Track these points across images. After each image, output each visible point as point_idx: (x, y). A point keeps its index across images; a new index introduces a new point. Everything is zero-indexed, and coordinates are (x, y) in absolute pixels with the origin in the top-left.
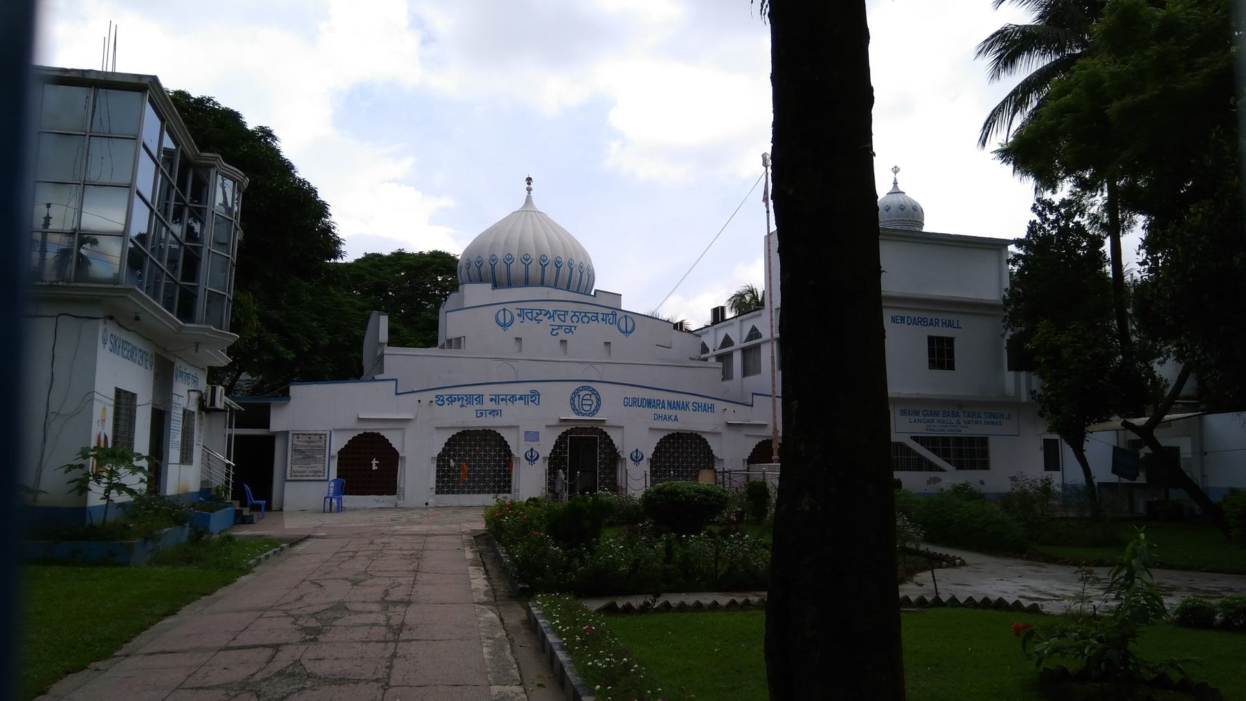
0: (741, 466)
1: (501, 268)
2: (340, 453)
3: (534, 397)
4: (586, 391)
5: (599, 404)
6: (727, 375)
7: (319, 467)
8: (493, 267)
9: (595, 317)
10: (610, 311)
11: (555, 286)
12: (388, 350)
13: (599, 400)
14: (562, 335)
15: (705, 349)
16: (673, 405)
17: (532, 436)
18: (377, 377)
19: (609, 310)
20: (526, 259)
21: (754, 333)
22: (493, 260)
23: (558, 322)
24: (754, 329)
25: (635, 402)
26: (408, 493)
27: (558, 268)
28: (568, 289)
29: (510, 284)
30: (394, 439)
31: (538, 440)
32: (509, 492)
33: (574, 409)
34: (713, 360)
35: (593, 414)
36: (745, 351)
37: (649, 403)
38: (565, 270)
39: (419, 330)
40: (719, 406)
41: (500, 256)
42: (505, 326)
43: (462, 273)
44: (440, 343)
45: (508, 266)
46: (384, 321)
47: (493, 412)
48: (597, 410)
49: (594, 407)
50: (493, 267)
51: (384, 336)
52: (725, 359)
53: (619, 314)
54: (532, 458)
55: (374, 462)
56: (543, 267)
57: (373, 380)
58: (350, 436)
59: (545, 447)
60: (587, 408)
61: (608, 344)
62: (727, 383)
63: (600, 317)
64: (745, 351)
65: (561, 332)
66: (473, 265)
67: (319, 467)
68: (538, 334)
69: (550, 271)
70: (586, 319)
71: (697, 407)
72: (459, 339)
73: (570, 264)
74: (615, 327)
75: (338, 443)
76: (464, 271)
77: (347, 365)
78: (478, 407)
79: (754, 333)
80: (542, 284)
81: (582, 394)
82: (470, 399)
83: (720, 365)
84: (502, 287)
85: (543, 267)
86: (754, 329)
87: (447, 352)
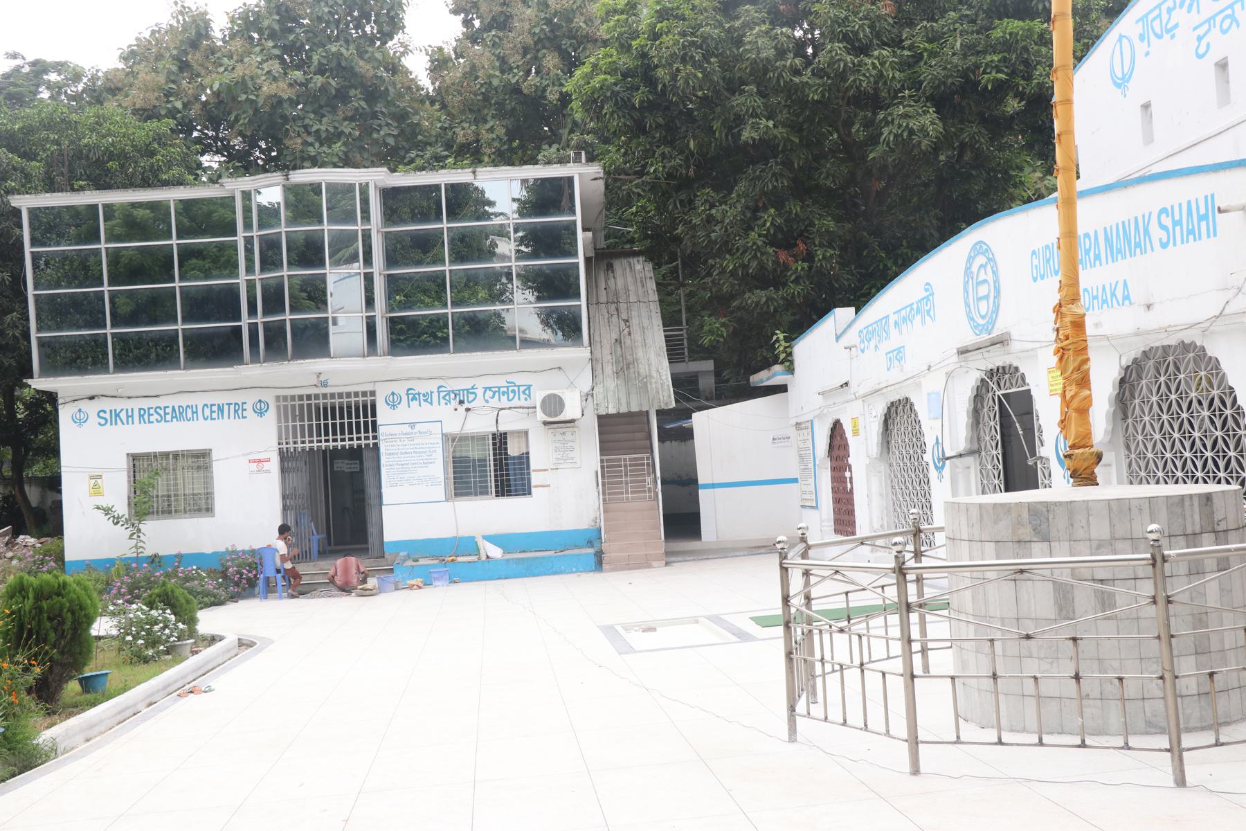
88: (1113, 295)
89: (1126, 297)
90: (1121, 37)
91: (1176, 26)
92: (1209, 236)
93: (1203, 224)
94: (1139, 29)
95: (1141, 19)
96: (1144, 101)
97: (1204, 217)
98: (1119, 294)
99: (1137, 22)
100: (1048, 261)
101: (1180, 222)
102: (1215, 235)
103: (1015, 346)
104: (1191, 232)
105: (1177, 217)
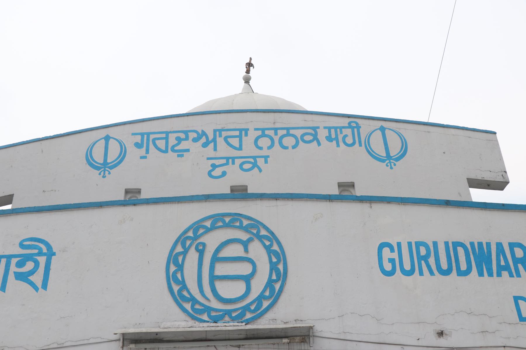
5: (279, 275)
10: (345, 122)
23: (223, 150)
25: (422, 259)
33: (180, 296)
42: (104, 167)
48: (274, 291)
49: (258, 285)
53: (366, 127)
60: (231, 290)
63: (322, 134)
70: (289, 141)
74: (360, 151)
81: (212, 240)
90: (107, 138)
91: (188, 150)
94: (138, 139)
95: (142, 135)
96: (131, 186)
100: (425, 258)
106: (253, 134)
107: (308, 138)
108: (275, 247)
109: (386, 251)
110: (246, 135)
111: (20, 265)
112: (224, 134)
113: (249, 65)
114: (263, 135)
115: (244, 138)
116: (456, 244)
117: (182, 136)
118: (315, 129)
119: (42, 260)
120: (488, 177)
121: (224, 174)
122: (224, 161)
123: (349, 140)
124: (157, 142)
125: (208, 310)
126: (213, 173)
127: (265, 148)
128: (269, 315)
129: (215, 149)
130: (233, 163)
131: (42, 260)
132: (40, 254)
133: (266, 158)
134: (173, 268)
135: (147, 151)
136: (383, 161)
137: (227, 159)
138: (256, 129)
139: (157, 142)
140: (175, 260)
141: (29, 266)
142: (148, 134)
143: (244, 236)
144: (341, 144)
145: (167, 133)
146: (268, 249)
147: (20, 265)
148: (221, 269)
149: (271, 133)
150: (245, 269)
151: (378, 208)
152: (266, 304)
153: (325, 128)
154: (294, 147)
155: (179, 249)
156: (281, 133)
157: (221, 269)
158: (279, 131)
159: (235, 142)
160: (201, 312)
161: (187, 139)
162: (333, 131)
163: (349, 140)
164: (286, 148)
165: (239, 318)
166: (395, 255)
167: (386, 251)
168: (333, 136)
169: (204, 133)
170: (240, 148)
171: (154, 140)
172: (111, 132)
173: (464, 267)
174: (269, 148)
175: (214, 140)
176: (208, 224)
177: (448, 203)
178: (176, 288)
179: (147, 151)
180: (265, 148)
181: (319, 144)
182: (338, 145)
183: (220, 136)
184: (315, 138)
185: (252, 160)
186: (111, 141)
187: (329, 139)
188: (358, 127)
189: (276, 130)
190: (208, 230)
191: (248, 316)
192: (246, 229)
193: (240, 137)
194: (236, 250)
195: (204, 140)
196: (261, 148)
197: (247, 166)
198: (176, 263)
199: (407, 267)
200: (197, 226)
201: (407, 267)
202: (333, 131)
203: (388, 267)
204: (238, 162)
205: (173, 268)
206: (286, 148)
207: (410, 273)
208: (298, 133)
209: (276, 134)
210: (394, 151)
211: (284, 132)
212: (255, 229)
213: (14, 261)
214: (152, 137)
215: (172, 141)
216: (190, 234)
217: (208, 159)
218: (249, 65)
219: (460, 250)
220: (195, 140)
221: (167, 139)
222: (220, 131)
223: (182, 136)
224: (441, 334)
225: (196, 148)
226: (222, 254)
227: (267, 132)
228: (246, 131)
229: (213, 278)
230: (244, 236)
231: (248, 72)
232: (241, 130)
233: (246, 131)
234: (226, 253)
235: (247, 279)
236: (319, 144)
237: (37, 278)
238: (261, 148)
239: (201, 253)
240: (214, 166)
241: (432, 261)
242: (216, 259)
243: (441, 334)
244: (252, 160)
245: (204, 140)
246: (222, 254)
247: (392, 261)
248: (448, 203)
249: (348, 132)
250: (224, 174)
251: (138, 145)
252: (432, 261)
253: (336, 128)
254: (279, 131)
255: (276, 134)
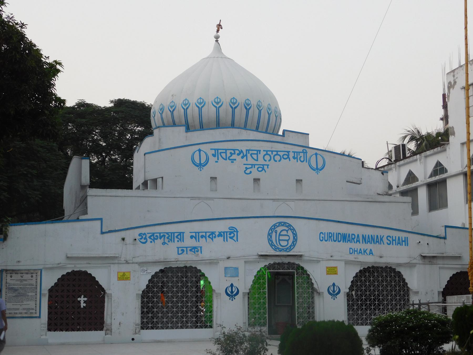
0: (437, 298)
1: (193, 112)
2: (50, 291)
3: (232, 233)
4: (283, 225)
5: (295, 239)
6: (415, 211)
7: (31, 304)
8: (185, 111)
9: (287, 156)
10: (300, 149)
11: (245, 127)
12: (92, 192)
13: (295, 235)
14: (255, 174)
15: (390, 187)
16: (365, 239)
17: (234, 272)
18: (82, 217)
19: (299, 148)
20: (218, 103)
21: (439, 169)
22: (186, 105)
24: (439, 164)
25: (330, 237)
26: (115, 327)
27: (248, 110)
28: (257, 129)
29: (202, 127)
30: (101, 275)
31: (238, 276)
32: (211, 327)
33: (272, 245)
34: (398, 195)
35: (290, 249)
36: (430, 186)
37: (345, 238)
38: (254, 112)
39: (114, 176)
40: (413, 239)
41: (193, 100)
42: (200, 166)
43: (155, 120)
44: (135, 186)
45: (200, 110)
46: (86, 164)
47: (194, 249)
48: (294, 244)
50: (185, 111)
51: (86, 178)
52: (411, 193)
53: (310, 152)
54: (232, 293)
55: (82, 299)
56: (234, 109)
57: (78, 220)
58: (58, 275)
59: (245, 282)
61: (299, 181)
62: (415, 217)
63: (291, 155)
64: (430, 186)
65: (254, 170)
66: (166, 110)
67: (31, 304)
68: (232, 173)
69: (240, 114)
70: (277, 158)
71: (391, 241)
72: (155, 181)
73: (259, 106)
74: (306, 164)
75: (49, 280)
76: (158, 116)
77: (49, 209)
78: (180, 244)
79: (439, 169)
80: (233, 125)
81: (279, 229)
82: (171, 237)
83: (408, 199)
84: (195, 130)
85: (234, 109)
86: (439, 164)
87: (141, 193)
88: (365, 251)
89: (372, 253)
91: (235, 160)
92: (405, 245)
93: (404, 243)
94: (213, 152)
95: (215, 149)
97: (405, 241)
98: (368, 252)
99: (211, 149)
100: (331, 237)
101: (395, 240)
102: (408, 245)
103: (304, 258)
104: (398, 243)
105: (394, 239)
106: (263, 153)
107: (285, 157)
108: (294, 232)
109: (321, 234)
110: (260, 153)
111: (230, 234)
112: (251, 152)
113: (219, 26)
114: (267, 154)
115: (259, 155)
116: (339, 233)
117: (233, 152)
118: (288, 152)
119: (235, 233)
120: (355, 180)
121: (251, 172)
122: (250, 166)
123: (302, 159)
124: (222, 154)
125: (278, 248)
126: (247, 172)
127: (267, 161)
128: (293, 250)
129: (247, 160)
130: (254, 167)
131: (235, 233)
132: (235, 231)
133: (268, 165)
134: (269, 237)
135: (218, 159)
136: (314, 170)
137: (252, 165)
138: (264, 151)
139: (222, 154)
140: (270, 235)
141: (232, 235)
142: (218, 150)
143: (287, 229)
144: (299, 160)
145: (226, 150)
146: (293, 232)
147: (230, 234)
148: (281, 238)
149: (270, 153)
150: (287, 238)
151: (321, 222)
152: (292, 247)
153: (293, 152)
154: (279, 161)
155: (270, 232)
156: (275, 153)
157: (281, 238)
158: (273, 152)
159: (255, 157)
160: (277, 249)
161: (234, 154)
162: (296, 153)
163: (302, 159)
164: (276, 161)
165: (286, 251)
166: (323, 236)
167: (321, 234)
168: (296, 157)
169: (242, 151)
170: (257, 160)
171: (221, 153)
172: (201, 147)
173: (340, 240)
174: (269, 160)
175: (246, 155)
176: (277, 225)
177: (339, 222)
178: (270, 242)
179: (218, 159)
180: (267, 161)
181: (290, 160)
182: (297, 161)
183: (249, 153)
184: (288, 157)
185: (262, 166)
186: (202, 152)
187: (294, 158)
188: (306, 153)
189: (272, 151)
190: (278, 227)
191: (288, 250)
192: (287, 227)
193: (257, 154)
194: (284, 233)
195: (242, 155)
196: (266, 161)
197: (260, 169)
198: (270, 236)
199: (326, 239)
200: (274, 225)
201: (326, 239)
202: (296, 153)
203: (321, 239)
204: (256, 167)
205: (269, 237)
206: (276, 161)
207: (326, 241)
208: (281, 154)
209: (272, 154)
210: (320, 166)
211: (276, 153)
212: (289, 226)
213: (228, 233)
214: (220, 151)
215: (228, 155)
216: (273, 227)
217: (244, 164)
218: (219, 26)
219: (340, 235)
220: (238, 155)
221: (226, 153)
222: (249, 150)
223: (233, 152)
224: (332, 256)
225: (238, 158)
226: (282, 233)
227: (268, 153)
228: (260, 151)
229: (279, 240)
230: (287, 229)
231: (218, 31)
232: (257, 151)
233: (260, 151)
234: (282, 233)
235: (288, 241)
236: (290, 160)
237: (235, 238)
238: (266, 161)
239: (276, 233)
240: (247, 168)
241: (332, 238)
242: (280, 235)
243: (332, 256)
244: (262, 166)
245: (242, 155)
246: (282, 233)
247: (323, 237)
248: (339, 222)
249: (302, 154)
250: (251, 172)
251: (214, 155)
252: (332, 238)
253: (297, 152)
254: (273, 152)
255: (272, 154)
